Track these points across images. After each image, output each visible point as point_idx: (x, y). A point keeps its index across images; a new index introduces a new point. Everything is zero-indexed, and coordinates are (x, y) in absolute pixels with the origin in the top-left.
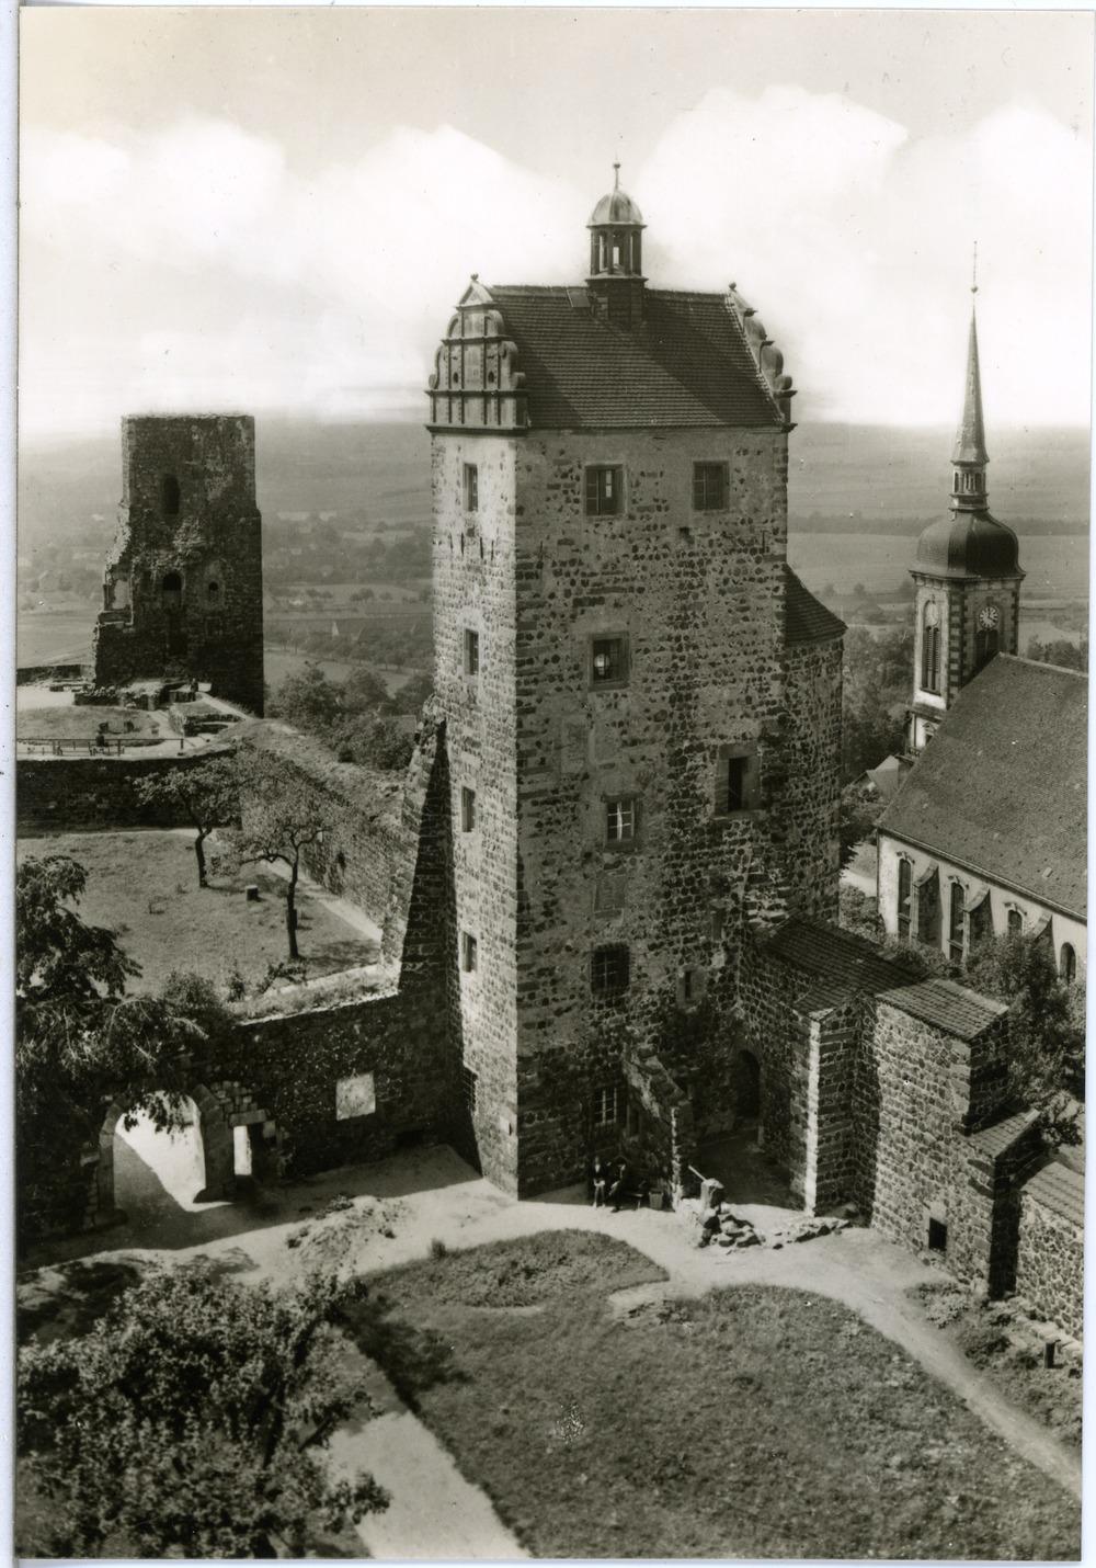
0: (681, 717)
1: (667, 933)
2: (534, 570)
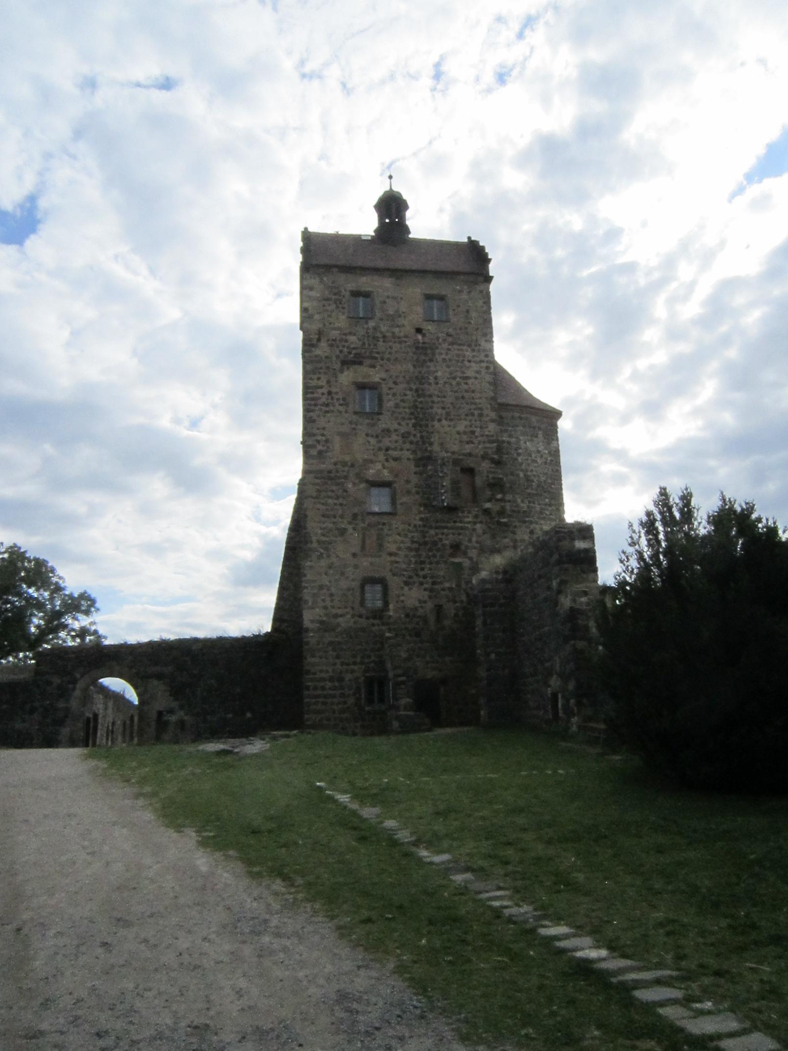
0: (422, 437)
1: (417, 575)
2: (315, 342)
